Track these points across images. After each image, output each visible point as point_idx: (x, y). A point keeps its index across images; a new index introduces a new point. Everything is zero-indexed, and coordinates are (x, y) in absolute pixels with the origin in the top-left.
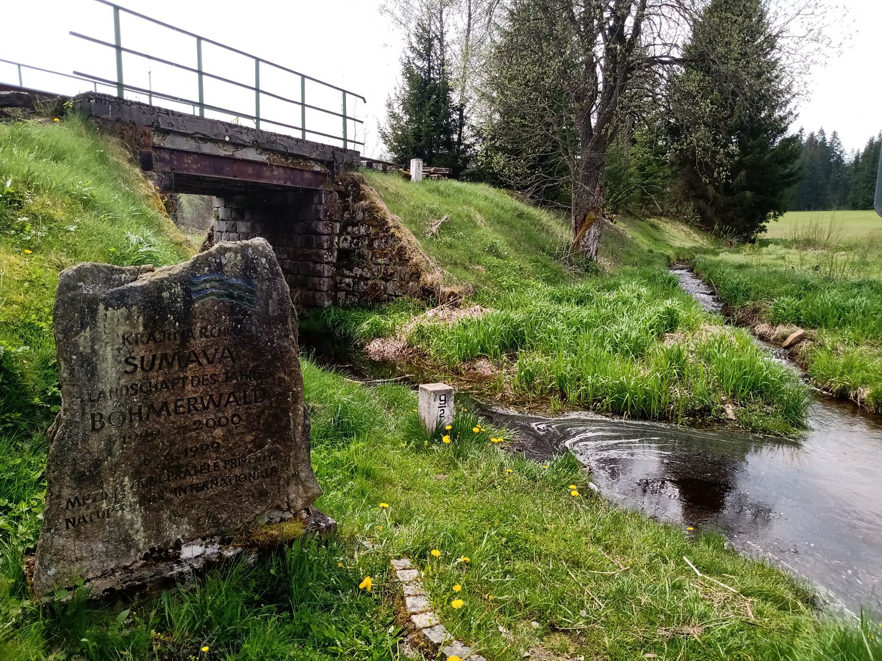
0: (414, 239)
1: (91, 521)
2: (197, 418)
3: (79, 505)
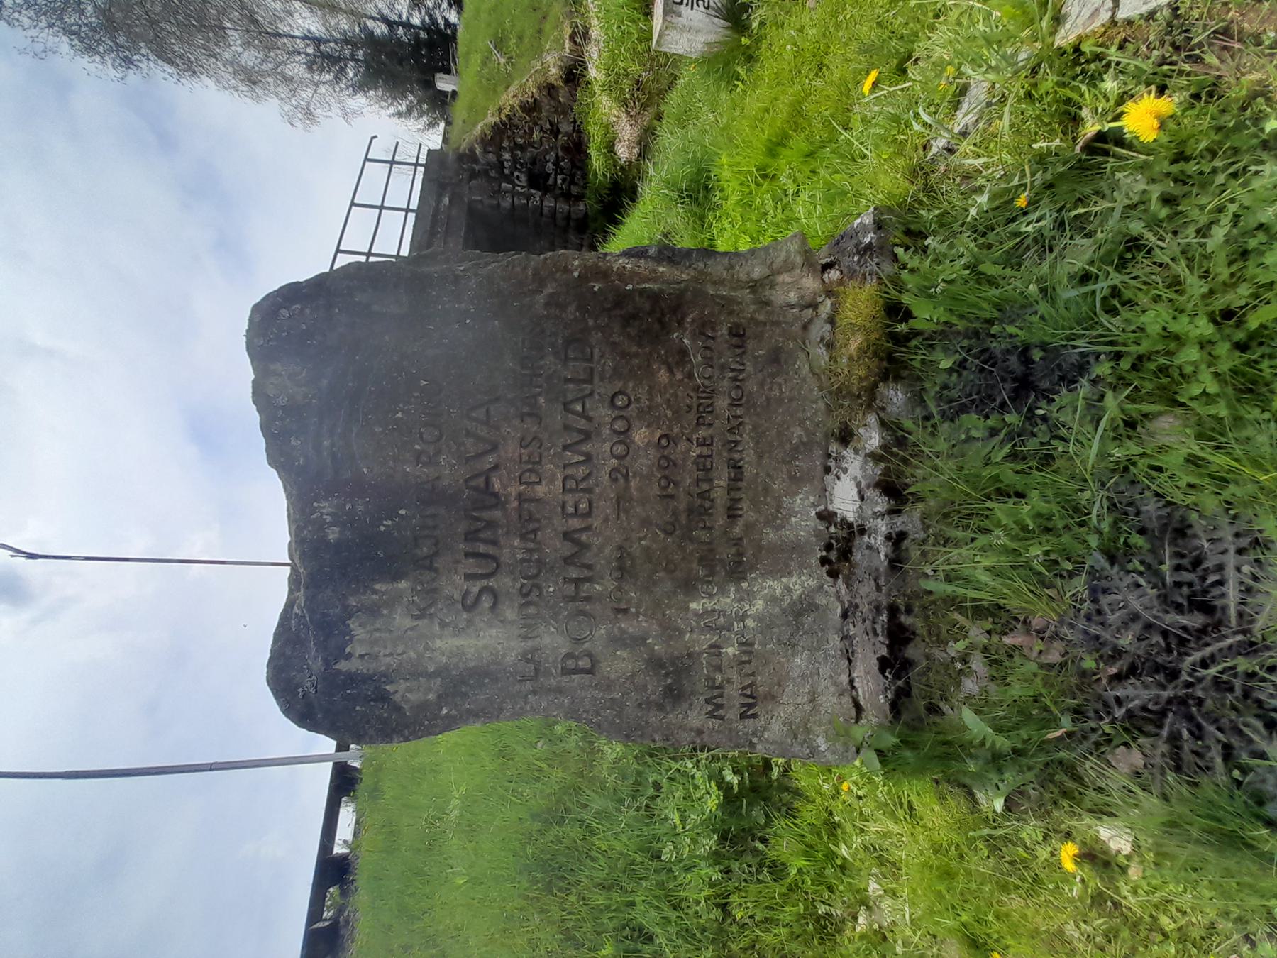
0: (512, 89)
1: (753, 674)
2: (604, 476)
3: (721, 696)
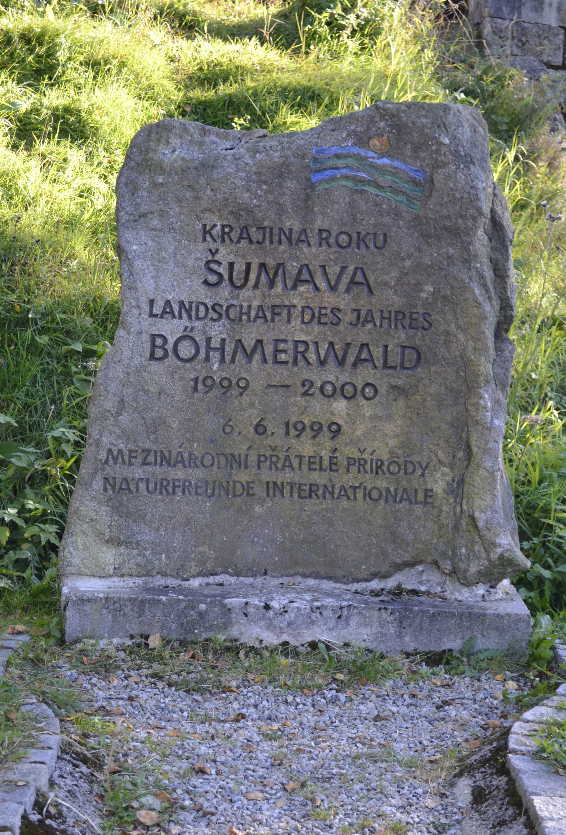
2: (305, 375)
3: (124, 463)
